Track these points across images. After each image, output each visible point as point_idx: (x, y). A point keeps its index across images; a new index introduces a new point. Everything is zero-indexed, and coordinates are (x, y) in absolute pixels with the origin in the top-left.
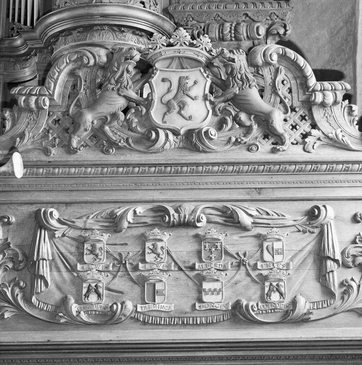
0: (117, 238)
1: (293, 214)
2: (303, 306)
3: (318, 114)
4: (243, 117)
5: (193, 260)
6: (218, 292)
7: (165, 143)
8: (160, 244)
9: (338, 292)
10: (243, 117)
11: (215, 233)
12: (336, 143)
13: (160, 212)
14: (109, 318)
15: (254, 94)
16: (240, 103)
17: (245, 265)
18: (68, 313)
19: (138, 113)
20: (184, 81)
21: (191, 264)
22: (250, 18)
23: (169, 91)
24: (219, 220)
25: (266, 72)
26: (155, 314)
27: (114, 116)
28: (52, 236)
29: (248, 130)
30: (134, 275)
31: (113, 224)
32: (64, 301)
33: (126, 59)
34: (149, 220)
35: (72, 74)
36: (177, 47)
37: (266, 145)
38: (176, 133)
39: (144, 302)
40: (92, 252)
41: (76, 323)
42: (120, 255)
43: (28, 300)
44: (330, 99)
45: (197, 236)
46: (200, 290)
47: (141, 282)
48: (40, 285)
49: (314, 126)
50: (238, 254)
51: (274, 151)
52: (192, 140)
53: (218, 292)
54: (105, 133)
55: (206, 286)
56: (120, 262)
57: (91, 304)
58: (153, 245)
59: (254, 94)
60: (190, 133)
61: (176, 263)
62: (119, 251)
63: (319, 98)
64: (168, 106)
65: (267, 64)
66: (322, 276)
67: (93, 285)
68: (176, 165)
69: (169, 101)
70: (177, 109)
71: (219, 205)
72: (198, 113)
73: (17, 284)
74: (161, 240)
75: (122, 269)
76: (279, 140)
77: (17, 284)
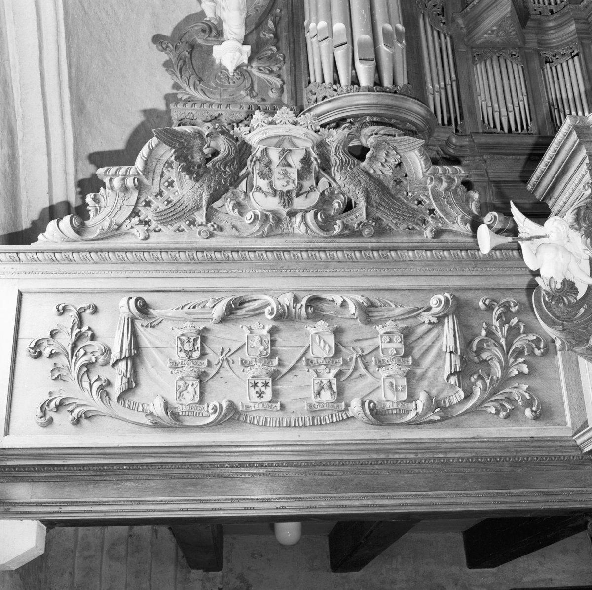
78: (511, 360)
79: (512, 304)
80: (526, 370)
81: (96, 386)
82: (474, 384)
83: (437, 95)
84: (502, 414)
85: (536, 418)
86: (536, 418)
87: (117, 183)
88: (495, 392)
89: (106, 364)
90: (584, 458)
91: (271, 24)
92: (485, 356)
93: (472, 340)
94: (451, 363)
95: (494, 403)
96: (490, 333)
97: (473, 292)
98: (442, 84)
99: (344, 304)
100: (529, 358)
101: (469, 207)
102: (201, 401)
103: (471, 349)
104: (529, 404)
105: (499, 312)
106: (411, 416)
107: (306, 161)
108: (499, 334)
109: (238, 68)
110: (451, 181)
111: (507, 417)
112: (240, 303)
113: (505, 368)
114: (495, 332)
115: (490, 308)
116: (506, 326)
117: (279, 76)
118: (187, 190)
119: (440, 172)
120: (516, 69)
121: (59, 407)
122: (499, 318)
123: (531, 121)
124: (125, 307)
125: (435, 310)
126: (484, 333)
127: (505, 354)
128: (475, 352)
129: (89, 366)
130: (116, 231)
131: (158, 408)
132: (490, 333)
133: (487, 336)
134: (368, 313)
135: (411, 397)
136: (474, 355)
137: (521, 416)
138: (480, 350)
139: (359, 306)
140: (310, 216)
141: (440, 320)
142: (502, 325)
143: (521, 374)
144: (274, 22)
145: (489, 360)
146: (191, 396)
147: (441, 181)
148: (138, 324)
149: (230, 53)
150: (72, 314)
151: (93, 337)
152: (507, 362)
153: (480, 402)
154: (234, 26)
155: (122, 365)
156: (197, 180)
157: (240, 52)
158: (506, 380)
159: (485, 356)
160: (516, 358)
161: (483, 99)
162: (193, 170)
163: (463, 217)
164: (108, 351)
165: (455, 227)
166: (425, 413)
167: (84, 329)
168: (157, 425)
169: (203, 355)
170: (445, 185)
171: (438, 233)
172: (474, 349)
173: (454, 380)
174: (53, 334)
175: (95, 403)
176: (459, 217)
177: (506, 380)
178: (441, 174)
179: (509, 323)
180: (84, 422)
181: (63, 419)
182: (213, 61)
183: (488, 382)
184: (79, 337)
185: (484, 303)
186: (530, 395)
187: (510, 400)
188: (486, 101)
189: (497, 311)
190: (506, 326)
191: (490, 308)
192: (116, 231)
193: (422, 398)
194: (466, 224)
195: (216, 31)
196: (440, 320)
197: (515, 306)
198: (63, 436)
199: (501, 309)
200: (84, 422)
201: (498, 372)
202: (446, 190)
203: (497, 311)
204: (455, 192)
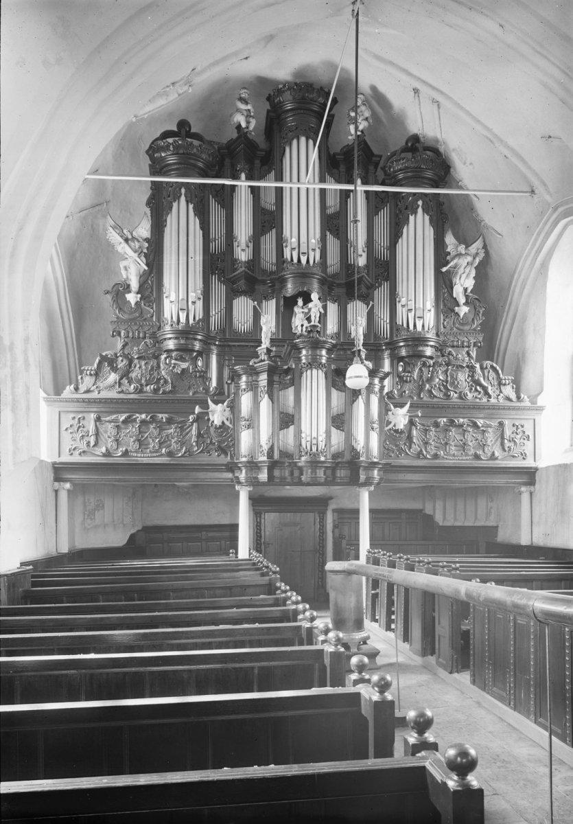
1: (495, 423)
2: (497, 454)
3: (502, 388)
4: (478, 388)
5: (462, 438)
9: (507, 449)
10: (478, 388)
12: (508, 399)
15: (482, 379)
16: (478, 383)
18: (423, 455)
19: (443, 385)
25: (486, 371)
28: (417, 429)
31: (437, 425)
32: (421, 450)
35: (420, 369)
37: (485, 400)
38: (456, 393)
43: (409, 450)
44: (507, 382)
48: (413, 446)
49: (501, 392)
51: (488, 401)
54: (432, 392)
59: (482, 379)
60: (461, 392)
63: (504, 382)
65: (486, 368)
66: (502, 444)
73: (406, 445)
76: (490, 397)
77: (406, 445)
81: (85, 443)
87: (88, 372)
89: (88, 436)
91: (150, 282)
94: (194, 439)
99: (162, 418)
102: (117, 449)
106: (180, 455)
107: (152, 368)
109: (137, 303)
112: (129, 417)
117: (152, 308)
118: (113, 377)
121: (74, 449)
124: (93, 416)
125: (191, 421)
129: (83, 436)
130: (88, 391)
131: (104, 450)
134: (170, 421)
135: (182, 448)
139: (166, 418)
140: (152, 386)
141: (192, 425)
144: (151, 281)
146: (115, 447)
148: (98, 423)
149: (132, 298)
150: (77, 420)
151: (83, 427)
154: (134, 285)
155: (92, 437)
156: (115, 373)
157: (136, 297)
162: (115, 369)
164: (89, 431)
166: (185, 453)
167: (81, 424)
168: (104, 455)
169: (118, 433)
171: (194, 394)
173: (194, 444)
174: (71, 426)
175: (86, 449)
180: (82, 454)
181: (77, 452)
182: (126, 298)
184: (79, 427)
192: (88, 391)
193: (184, 449)
195: (128, 288)
196: (192, 423)
198: (77, 458)
200: (82, 454)
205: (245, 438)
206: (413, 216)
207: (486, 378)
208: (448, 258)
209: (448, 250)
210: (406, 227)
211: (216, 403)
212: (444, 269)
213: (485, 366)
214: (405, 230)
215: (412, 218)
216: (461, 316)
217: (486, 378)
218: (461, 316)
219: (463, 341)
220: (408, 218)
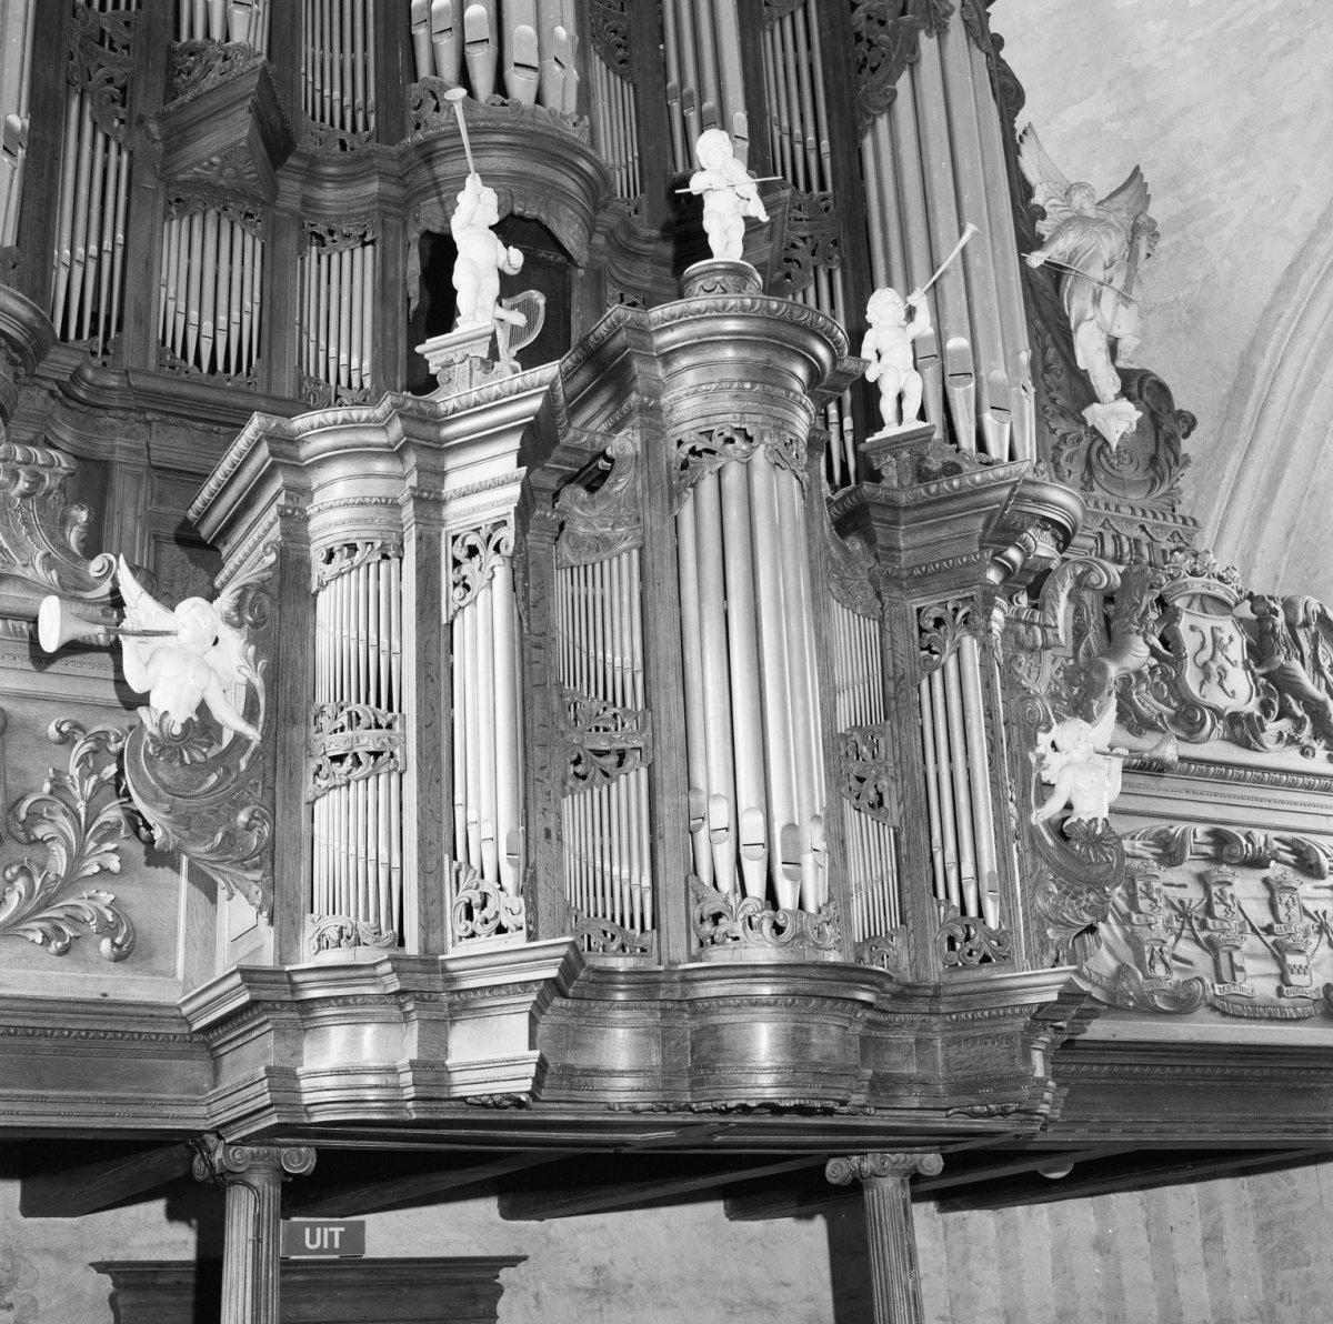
0: (1173, 875)
5: (1268, 919)
6: (1303, 970)
7: (1212, 730)
8: (1228, 891)
11: (1293, 878)
13: (1220, 839)
14: (1183, 1004)
17: (1327, 932)
20: (1219, 635)
21: (1265, 925)
22: (1147, 533)
23: (1203, 646)
24: (1291, 858)
26: (1237, 999)
27: (1139, 673)
29: (1299, 724)
30: (1202, 935)
33: (1152, 587)
34: (1209, 850)
36: (1204, 579)
39: (1220, 981)
40: (1148, 895)
41: (1147, 1010)
42: (1181, 902)
45: (1266, 881)
46: (1281, 962)
47: (1211, 946)
50: (1316, 912)
52: (1242, 730)
53: (1303, 970)
55: (1291, 959)
56: (1184, 913)
57: (1159, 979)
58: (1221, 891)
61: (1250, 924)
62: (1179, 896)
64: (1205, 667)
67: (1157, 948)
68: (1221, 764)
69: (1205, 663)
70: (1217, 679)
71: (1287, 835)
72: (1238, 690)
74: (1230, 884)
75: (1187, 926)
78: (92, 845)
79: (112, 738)
80: (114, 863)
82: (10, 882)
83: (78, 271)
84: (56, 945)
85: (119, 958)
86: (119, 958)
88: (46, 904)
90: (195, 1039)
92: (41, 831)
93: (23, 798)
95: (43, 924)
96: (59, 787)
97: (39, 704)
98: (93, 249)
100: (125, 845)
101: (64, 536)
103: (16, 816)
104: (108, 929)
105: (85, 749)
108: (77, 793)
110: (37, 480)
111: (64, 952)
113: (76, 858)
114: (71, 788)
115: (66, 740)
116: (94, 779)
119: (19, 458)
120: (249, 246)
122: (83, 760)
123: (258, 357)
126: (47, 787)
127: (82, 832)
128: (23, 822)
132: (59, 787)
133: (51, 793)
136: (20, 826)
137: (91, 953)
138: (35, 816)
142: (84, 777)
143: (104, 871)
145: (49, 840)
147: (15, 476)
152: (82, 847)
153: (15, 919)
158: (72, 880)
159: (41, 831)
160: (101, 842)
161: (171, 295)
163: (48, 555)
165: (29, 573)
170: (23, 485)
172: (23, 815)
176: (41, 553)
177: (72, 880)
178: (19, 463)
179: (99, 774)
183: (38, 882)
185: (59, 730)
186: (115, 915)
187: (74, 920)
188: (176, 299)
189: (81, 747)
190: (94, 779)
191: (66, 740)
194: (50, 569)
197: (116, 742)
199: (89, 745)
201: (59, 862)
202: (25, 496)
203: (81, 747)
204: (42, 504)
205: (348, 828)
206: (934, 41)
207: (1308, 661)
208: (1043, 227)
209: (1038, 199)
210: (905, 76)
211: (166, 592)
212: (1036, 259)
213: (1301, 617)
214: (903, 84)
215: (927, 44)
216: (1114, 446)
217: (1308, 661)
218: (1114, 446)
219: (1137, 541)
220: (914, 48)
